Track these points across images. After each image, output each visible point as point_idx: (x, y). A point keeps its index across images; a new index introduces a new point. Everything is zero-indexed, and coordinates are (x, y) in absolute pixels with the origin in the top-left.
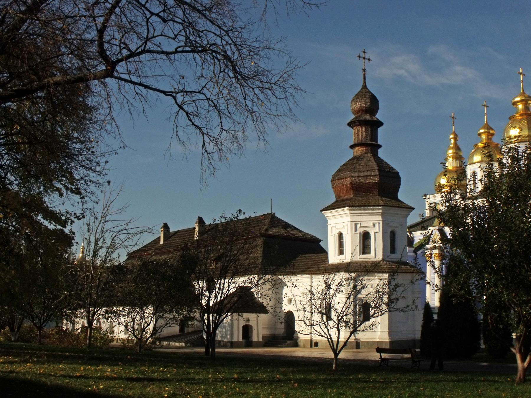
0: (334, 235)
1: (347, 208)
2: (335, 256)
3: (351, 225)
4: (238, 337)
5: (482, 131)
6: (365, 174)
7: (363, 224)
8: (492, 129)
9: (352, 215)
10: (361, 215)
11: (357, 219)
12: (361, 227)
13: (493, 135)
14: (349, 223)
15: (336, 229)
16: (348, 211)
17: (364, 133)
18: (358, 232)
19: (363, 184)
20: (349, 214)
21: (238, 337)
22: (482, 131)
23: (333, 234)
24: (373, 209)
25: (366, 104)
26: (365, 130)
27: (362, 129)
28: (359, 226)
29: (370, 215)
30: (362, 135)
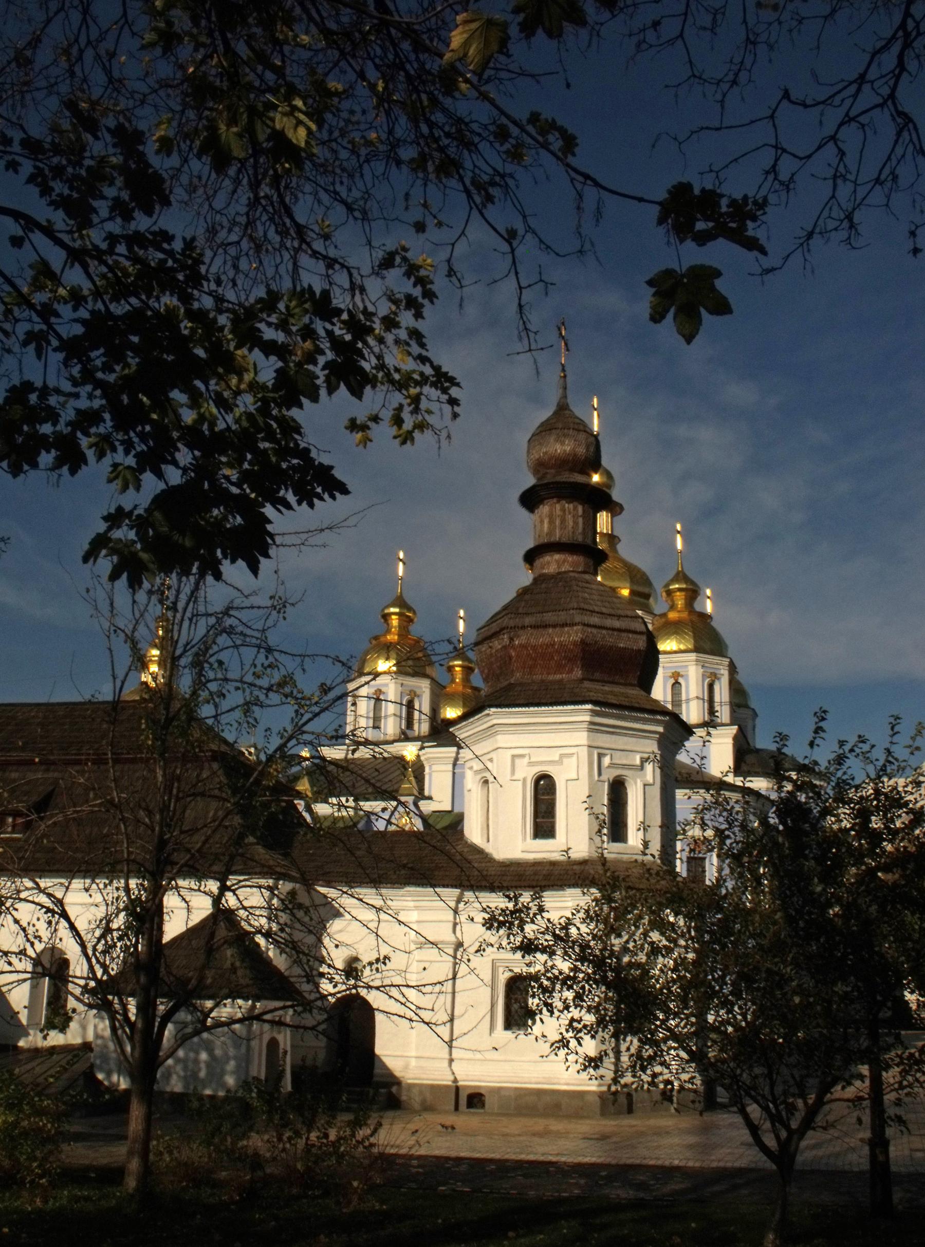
0: (525, 780)
1: (589, 706)
2: (524, 839)
3: (590, 756)
4: (259, 1071)
5: (392, 610)
6: (617, 624)
7: (620, 759)
8: (410, 609)
9: (593, 728)
10: (614, 731)
11: (605, 740)
12: (612, 765)
13: (410, 620)
14: (584, 752)
15: (531, 764)
16: (587, 718)
17: (580, 520)
18: (605, 777)
19: (611, 648)
20: (585, 725)
21: (259, 1071)
22: (392, 610)
23: (519, 775)
24: (645, 721)
25: (587, 450)
26: (584, 511)
27: (575, 508)
28: (606, 761)
29: (632, 736)
30: (576, 523)
